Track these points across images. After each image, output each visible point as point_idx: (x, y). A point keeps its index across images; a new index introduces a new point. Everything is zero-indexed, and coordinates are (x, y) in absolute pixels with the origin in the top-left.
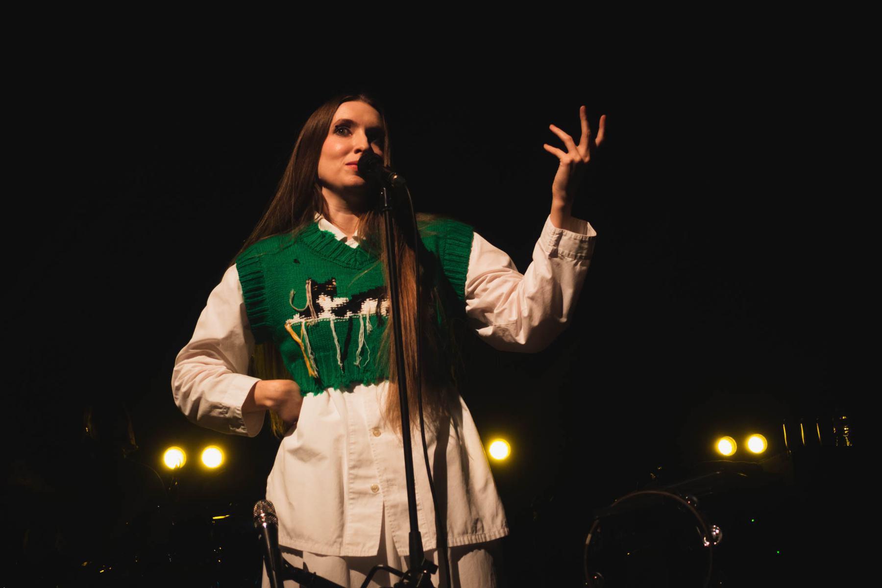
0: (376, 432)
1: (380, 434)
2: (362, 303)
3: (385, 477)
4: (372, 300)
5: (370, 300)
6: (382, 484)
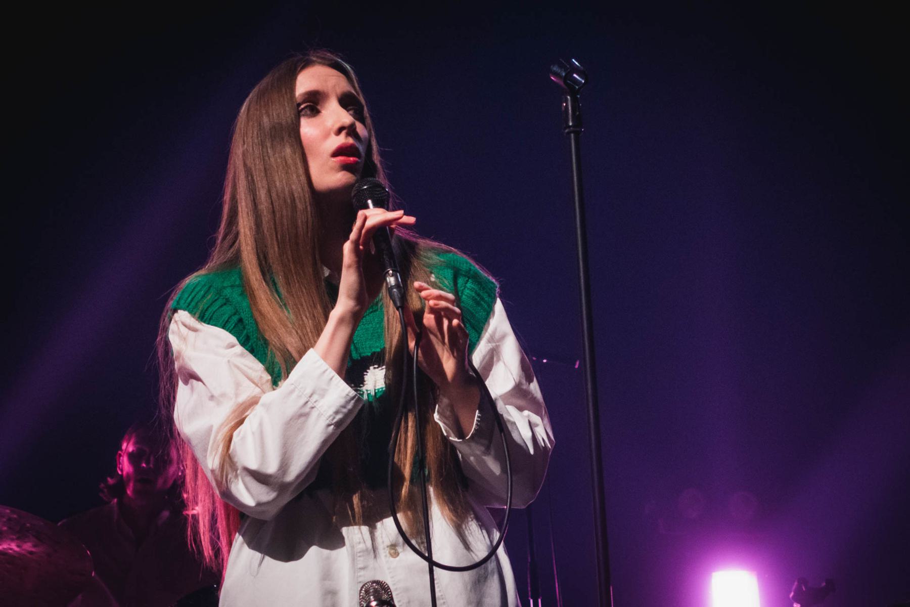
0: (392, 551)
1: (398, 554)
2: (365, 373)
4: (378, 368)
5: (375, 368)
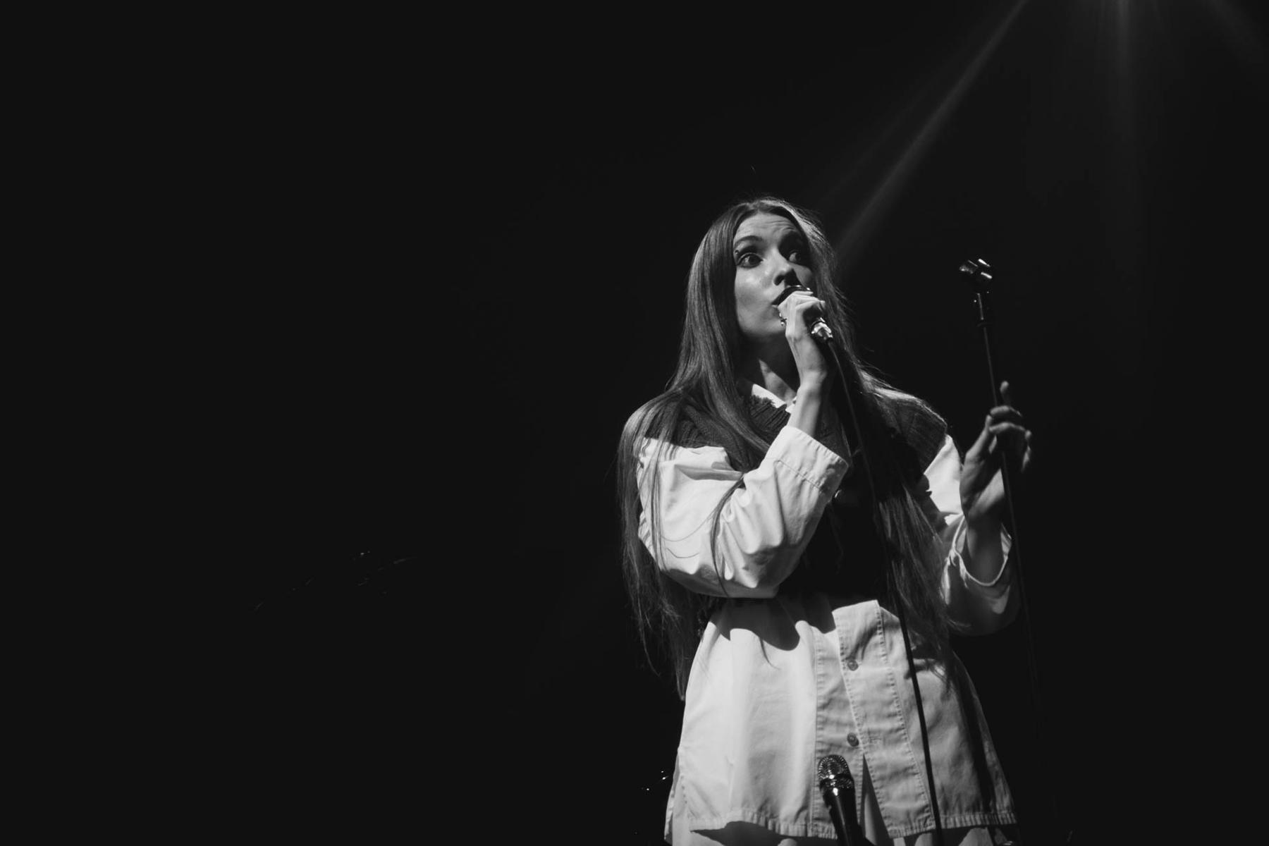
0: (851, 663)
3: (865, 727)
6: (862, 736)
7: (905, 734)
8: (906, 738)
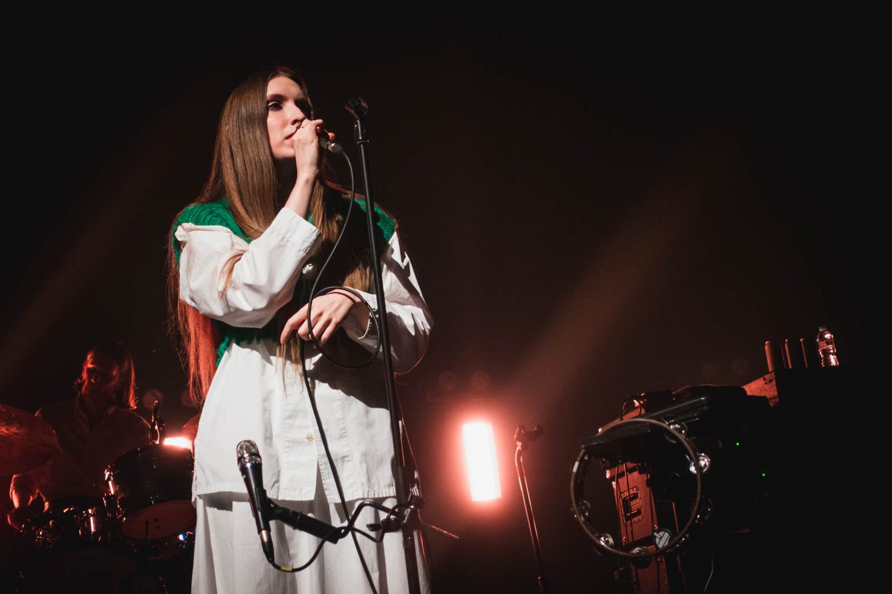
7: (345, 433)
8: (346, 436)
